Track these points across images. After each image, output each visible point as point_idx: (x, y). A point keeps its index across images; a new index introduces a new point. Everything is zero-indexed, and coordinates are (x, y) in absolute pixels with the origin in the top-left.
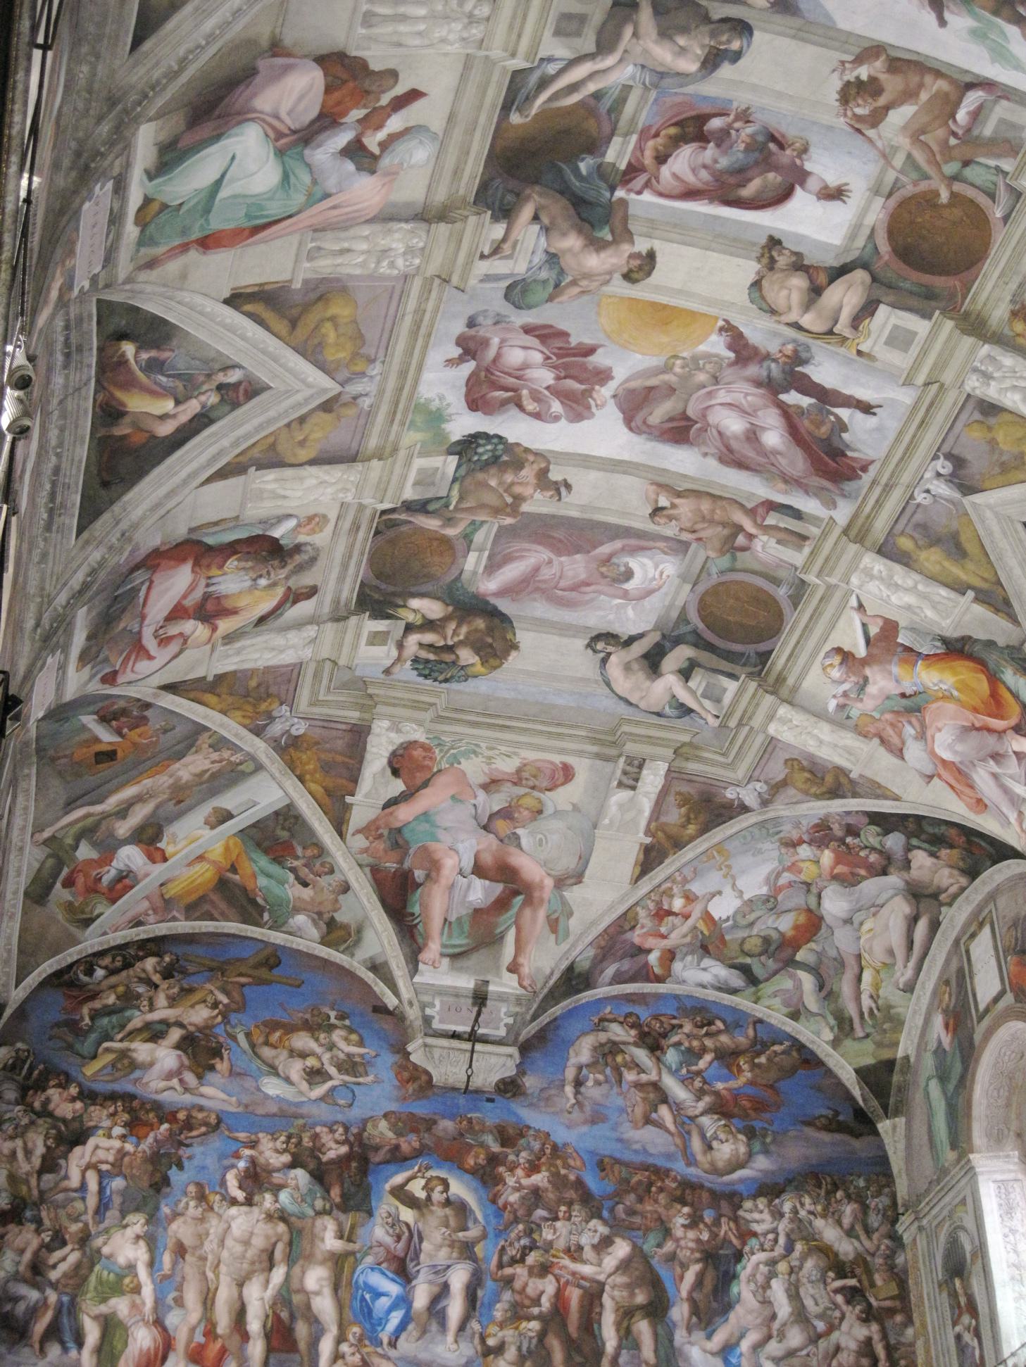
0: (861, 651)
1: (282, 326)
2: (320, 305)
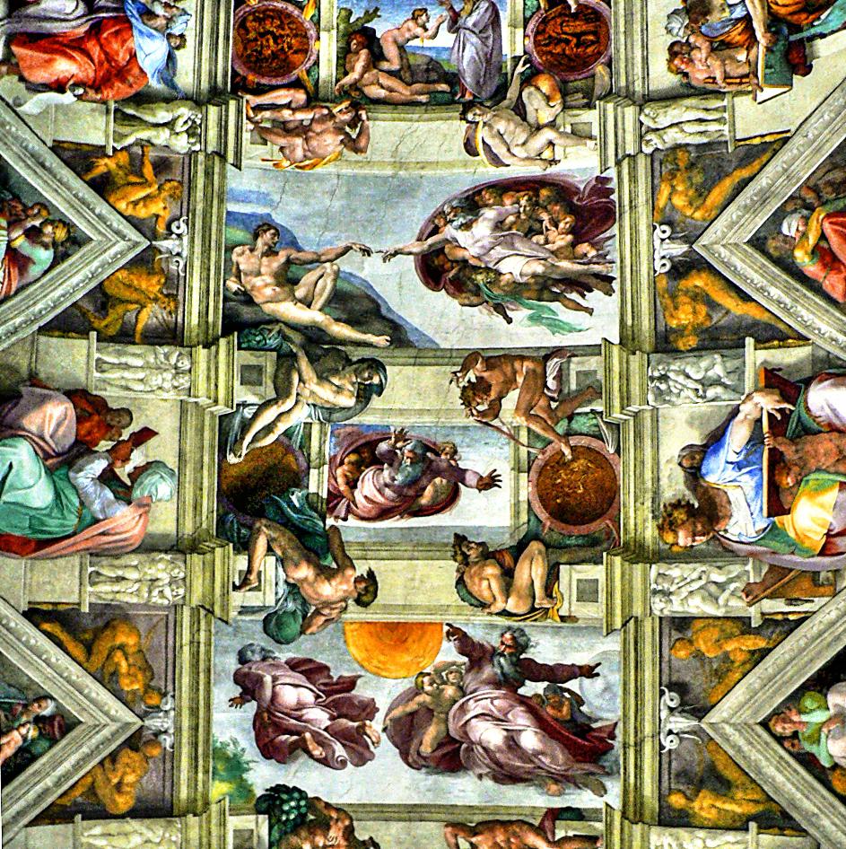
1: (78, 651)
2: (108, 632)
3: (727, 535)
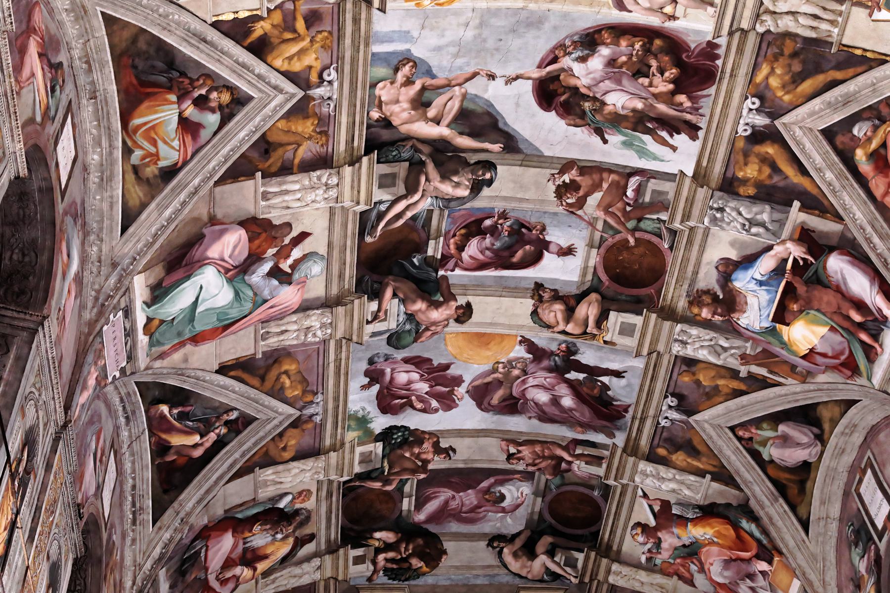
0: (652, 522)
1: (256, 382)
2: (276, 365)
3: (739, 322)
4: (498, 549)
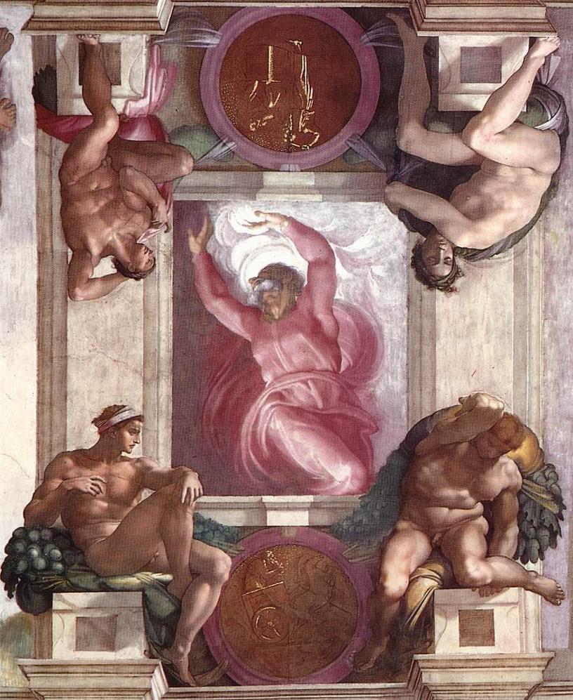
4: (460, 262)
